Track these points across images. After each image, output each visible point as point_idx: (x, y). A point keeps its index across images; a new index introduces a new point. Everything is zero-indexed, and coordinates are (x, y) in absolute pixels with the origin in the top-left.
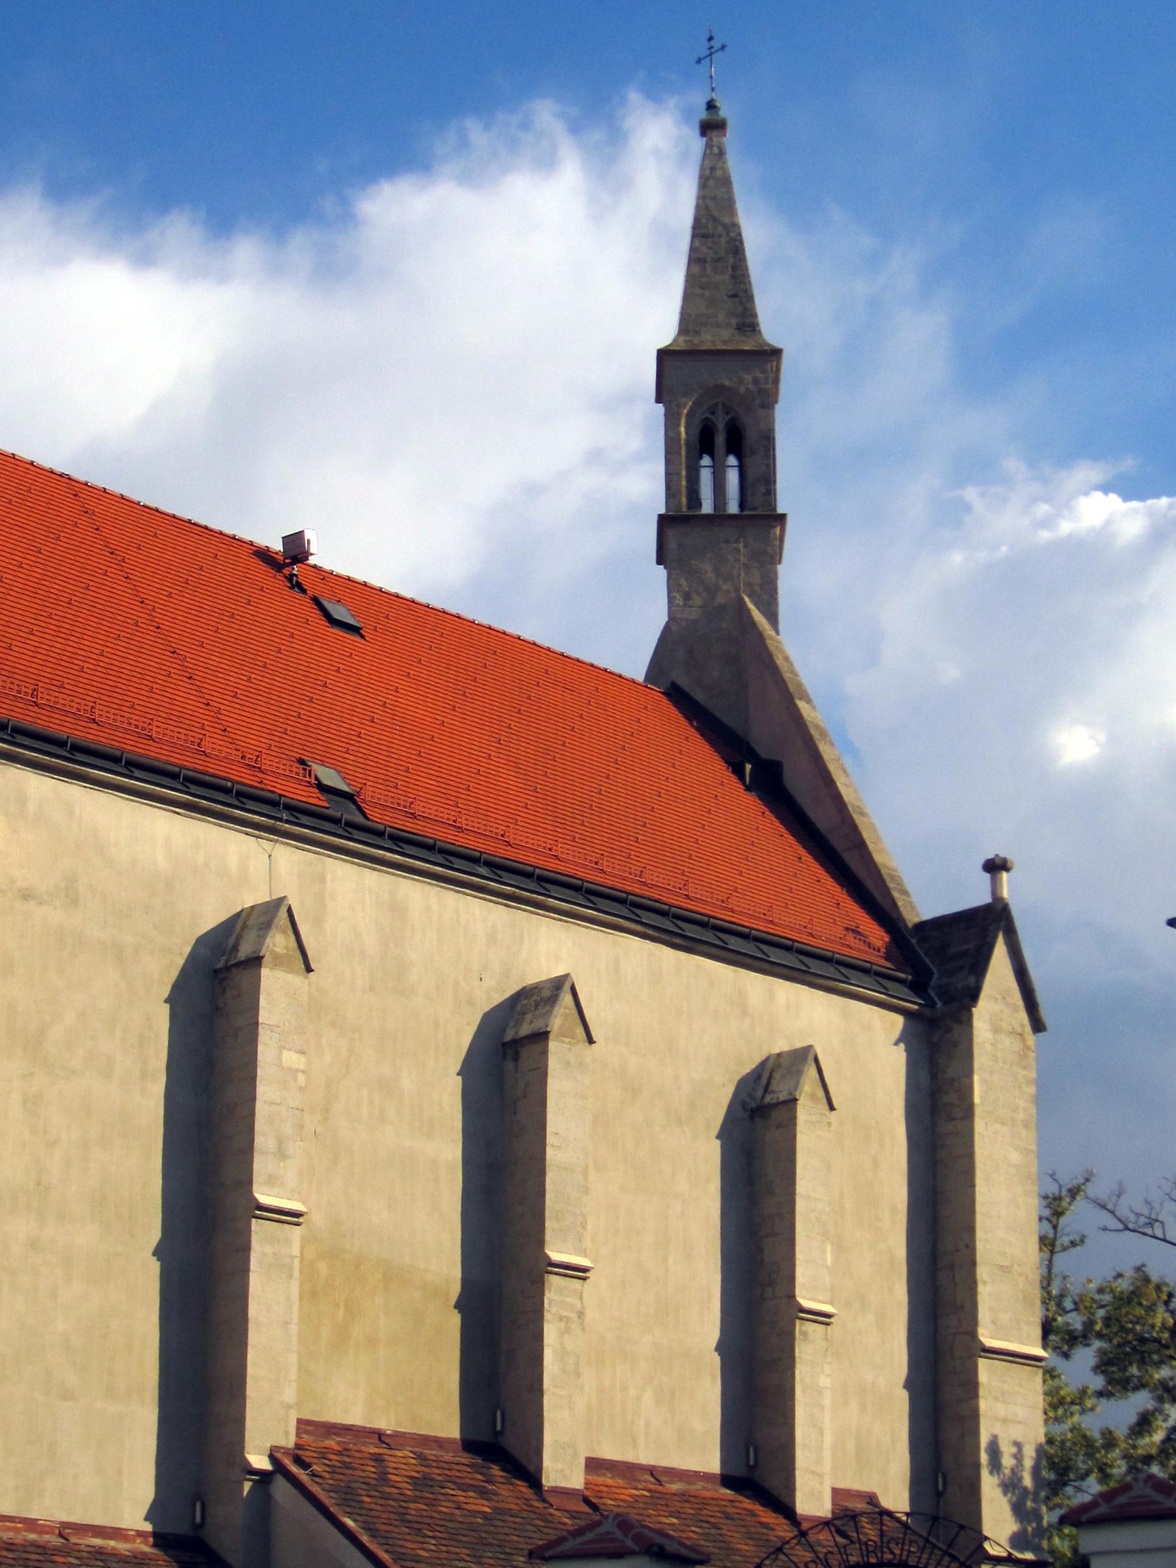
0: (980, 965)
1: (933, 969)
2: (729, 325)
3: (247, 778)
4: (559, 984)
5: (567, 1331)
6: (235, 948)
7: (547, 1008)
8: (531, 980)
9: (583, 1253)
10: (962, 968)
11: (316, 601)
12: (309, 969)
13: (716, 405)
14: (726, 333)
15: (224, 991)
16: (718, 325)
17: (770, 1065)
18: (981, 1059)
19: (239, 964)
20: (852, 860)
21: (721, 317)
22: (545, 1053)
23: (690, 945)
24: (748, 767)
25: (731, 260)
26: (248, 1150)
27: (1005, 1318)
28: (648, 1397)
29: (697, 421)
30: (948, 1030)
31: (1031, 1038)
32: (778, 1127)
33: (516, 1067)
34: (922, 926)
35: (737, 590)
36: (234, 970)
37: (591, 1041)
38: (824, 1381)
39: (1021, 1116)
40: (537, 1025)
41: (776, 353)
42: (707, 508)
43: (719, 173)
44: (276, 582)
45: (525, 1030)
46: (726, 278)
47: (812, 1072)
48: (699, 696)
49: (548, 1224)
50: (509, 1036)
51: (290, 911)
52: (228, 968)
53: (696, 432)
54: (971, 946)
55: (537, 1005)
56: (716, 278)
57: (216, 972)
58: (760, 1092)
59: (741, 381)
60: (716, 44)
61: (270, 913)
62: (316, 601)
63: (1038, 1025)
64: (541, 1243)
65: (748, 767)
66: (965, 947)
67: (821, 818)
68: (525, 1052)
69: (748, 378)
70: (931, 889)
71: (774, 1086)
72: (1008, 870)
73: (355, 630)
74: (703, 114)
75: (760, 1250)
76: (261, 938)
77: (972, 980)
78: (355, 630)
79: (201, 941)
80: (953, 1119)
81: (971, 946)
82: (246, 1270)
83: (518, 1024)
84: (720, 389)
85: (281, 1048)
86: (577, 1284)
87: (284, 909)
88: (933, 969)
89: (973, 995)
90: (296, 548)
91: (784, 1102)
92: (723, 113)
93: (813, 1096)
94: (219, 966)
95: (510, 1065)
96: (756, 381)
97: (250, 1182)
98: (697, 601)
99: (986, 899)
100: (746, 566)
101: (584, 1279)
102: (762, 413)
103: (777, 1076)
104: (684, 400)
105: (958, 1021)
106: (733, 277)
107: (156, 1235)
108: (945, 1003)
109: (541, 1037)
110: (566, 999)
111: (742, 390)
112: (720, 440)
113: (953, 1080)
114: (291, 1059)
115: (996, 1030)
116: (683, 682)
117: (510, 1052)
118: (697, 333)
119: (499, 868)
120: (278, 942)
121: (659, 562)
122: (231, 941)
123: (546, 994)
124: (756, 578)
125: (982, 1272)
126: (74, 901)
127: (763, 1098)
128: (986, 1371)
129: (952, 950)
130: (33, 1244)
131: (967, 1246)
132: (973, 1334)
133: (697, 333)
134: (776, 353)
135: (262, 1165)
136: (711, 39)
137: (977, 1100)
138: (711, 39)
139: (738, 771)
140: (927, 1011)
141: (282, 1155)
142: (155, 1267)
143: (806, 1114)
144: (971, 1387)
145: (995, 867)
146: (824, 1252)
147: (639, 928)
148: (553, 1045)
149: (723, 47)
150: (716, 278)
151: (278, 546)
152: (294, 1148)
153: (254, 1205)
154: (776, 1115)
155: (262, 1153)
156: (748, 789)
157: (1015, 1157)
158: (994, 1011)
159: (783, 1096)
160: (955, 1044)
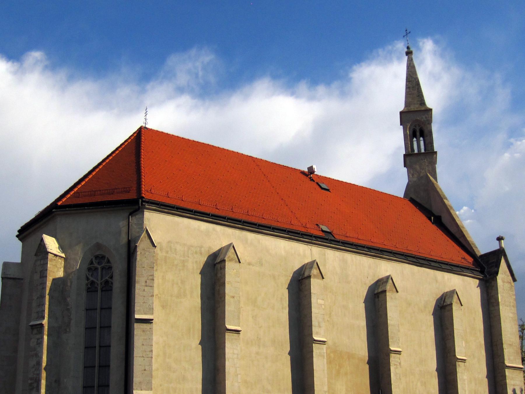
0: (498, 265)
1: (486, 267)
3: (303, 230)
4: (388, 278)
5: (396, 368)
6: (304, 274)
8: (381, 277)
9: (400, 347)
11: (317, 183)
12: (323, 278)
14: (417, 106)
16: (414, 104)
17: (444, 295)
18: (500, 290)
19: (305, 278)
20: (461, 240)
22: (386, 295)
23: (421, 265)
24: (432, 218)
25: (417, 87)
26: (311, 326)
27: (512, 358)
28: (419, 384)
29: (411, 129)
31: (513, 284)
34: (482, 256)
35: (426, 172)
37: (397, 292)
38: (465, 377)
39: (512, 304)
40: (383, 289)
41: (431, 110)
42: (416, 151)
43: (412, 65)
44: (307, 179)
45: (380, 290)
46: (416, 92)
47: (456, 296)
48: (418, 200)
49: (390, 340)
50: (376, 292)
51: (317, 263)
52: (302, 279)
53: (412, 132)
57: (299, 280)
58: (442, 302)
59: (422, 118)
60: (408, 31)
61: (312, 264)
62: (317, 183)
63: (514, 280)
64: (388, 345)
65: (432, 218)
67: (453, 230)
68: (380, 296)
69: (424, 117)
70: (483, 246)
71: (446, 300)
72: (503, 240)
73: (328, 190)
76: (310, 271)
77: (496, 269)
78: (328, 190)
82: (312, 357)
83: (378, 289)
84: (417, 120)
85: (317, 299)
86: (398, 355)
87: (315, 263)
88: (486, 267)
89: (497, 273)
90: (311, 170)
92: (411, 49)
93: (456, 303)
95: (377, 300)
96: (426, 118)
97: (312, 334)
98: (415, 176)
99: (498, 247)
102: (428, 125)
103: (447, 298)
106: (418, 91)
107: (288, 349)
109: (385, 292)
110: (390, 281)
111: (423, 120)
112: (418, 134)
114: (320, 301)
115: (503, 282)
116: (414, 197)
118: (410, 106)
119: (370, 249)
120: (315, 271)
121: (405, 166)
122: (303, 272)
123: (385, 280)
125: (505, 346)
126: (262, 265)
128: (508, 372)
130: (257, 353)
132: (504, 363)
134: (431, 110)
135: (315, 330)
137: (500, 301)
139: (430, 219)
140: (485, 278)
141: (320, 327)
142: (289, 357)
143: (455, 307)
144: (504, 377)
145: (500, 239)
146: (462, 343)
147: (408, 262)
148: (387, 294)
151: (306, 170)
152: (323, 324)
154: (448, 308)
155: (315, 326)
156: (433, 223)
157: (511, 315)
158: (502, 277)
159: (449, 303)
160: (493, 286)
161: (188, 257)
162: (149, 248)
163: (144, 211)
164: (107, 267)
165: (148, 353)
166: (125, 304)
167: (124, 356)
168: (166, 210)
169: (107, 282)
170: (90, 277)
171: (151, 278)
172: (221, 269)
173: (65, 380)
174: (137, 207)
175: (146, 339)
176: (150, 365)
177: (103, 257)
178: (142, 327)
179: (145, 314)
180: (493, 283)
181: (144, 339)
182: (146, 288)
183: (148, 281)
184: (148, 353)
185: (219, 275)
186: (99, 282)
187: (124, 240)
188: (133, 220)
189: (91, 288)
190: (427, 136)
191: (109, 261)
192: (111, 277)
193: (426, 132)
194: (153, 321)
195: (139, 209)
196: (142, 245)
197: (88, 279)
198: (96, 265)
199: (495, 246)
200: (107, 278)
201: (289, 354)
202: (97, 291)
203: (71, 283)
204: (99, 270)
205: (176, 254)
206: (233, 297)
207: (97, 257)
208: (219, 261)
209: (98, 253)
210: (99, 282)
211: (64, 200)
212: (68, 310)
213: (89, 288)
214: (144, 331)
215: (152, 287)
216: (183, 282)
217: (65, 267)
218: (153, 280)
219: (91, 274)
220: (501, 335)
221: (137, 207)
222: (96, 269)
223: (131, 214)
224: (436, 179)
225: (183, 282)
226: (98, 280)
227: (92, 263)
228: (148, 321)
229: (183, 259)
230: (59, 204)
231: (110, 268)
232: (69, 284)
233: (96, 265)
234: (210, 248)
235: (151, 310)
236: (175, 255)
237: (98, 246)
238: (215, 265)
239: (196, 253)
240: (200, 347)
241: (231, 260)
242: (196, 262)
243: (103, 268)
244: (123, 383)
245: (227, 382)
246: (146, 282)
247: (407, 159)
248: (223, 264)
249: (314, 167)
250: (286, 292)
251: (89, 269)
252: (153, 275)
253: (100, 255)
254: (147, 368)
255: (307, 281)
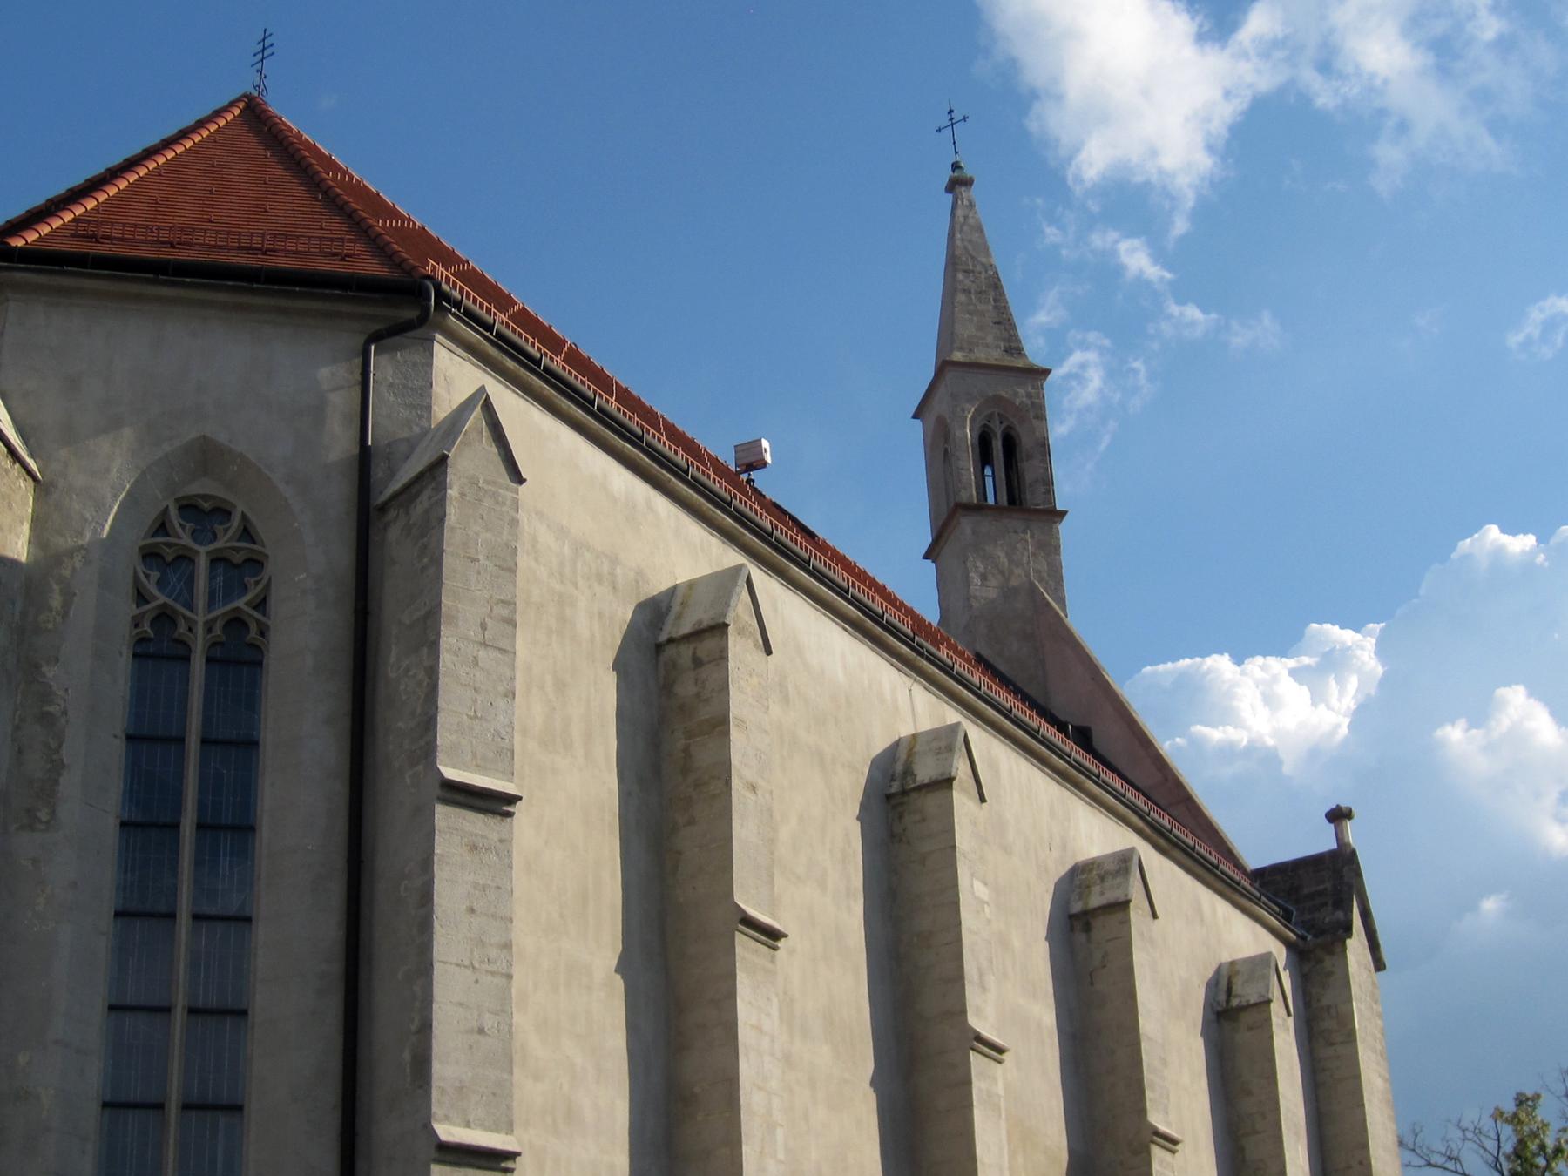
2: (998, 347)
6: (908, 772)
7: (1118, 880)
9: (1169, 1124)
10: (1325, 904)
12: (982, 799)
13: (992, 414)
15: (901, 817)
16: (987, 346)
17: (1225, 972)
21: (990, 339)
25: (992, 294)
26: (958, 978)
29: (977, 426)
30: (1321, 961)
32: (1250, 1029)
33: (1089, 940)
35: (1028, 575)
36: (914, 795)
37: (1155, 916)
42: (991, 501)
43: (971, 221)
45: (1095, 901)
49: (1148, 1093)
50: (1077, 907)
52: (905, 792)
53: (976, 437)
54: (1328, 885)
55: (1102, 879)
56: (980, 307)
57: (889, 797)
58: (1222, 997)
59: (1016, 394)
60: (957, 116)
64: (1142, 1111)
66: (1321, 887)
68: (1097, 923)
69: (1021, 392)
71: (1237, 989)
74: (947, 174)
75: (1241, 1149)
77: (1340, 915)
79: (875, 763)
80: (1332, 1044)
81: (1328, 885)
82: (969, 1106)
84: (997, 400)
91: (1256, 1005)
92: (968, 171)
94: (893, 790)
95: (1080, 937)
96: (1029, 395)
97: (964, 1012)
99: (1333, 845)
100: (1034, 554)
101: (1173, 1152)
102: (1036, 423)
104: (967, 406)
105: (1331, 953)
106: (996, 307)
108: (1315, 936)
112: (997, 446)
113: (1329, 1007)
116: (985, 653)
117: (1078, 925)
118: (971, 351)
122: (899, 768)
123: (1112, 867)
124: (1044, 567)
127: (1228, 1001)
129: (1306, 891)
131: (1361, 1163)
133: (971, 351)
135: (972, 996)
136: (951, 112)
138: (951, 112)
140: (1301, 943)
141: (983, 988)
147: (1140, 823)
149: (965, 119)
150: (980, 307)
152: (991, 980)
153: (972, 1036)
154: (1246, 1018)
159: (1253, 999)
160: (1330, 974)
161: (576, 585)
162: (494, 483)
163: (432, 339)
164: (238, 558)
165: (493, 953)
166: (345, 724)
167: (337, 968)
168: (510, 364)
169: (236, 622)
170: (154, 590)
171: (505, 612)
172: (697, 663)
173: (22, 1059)
174: (411, 314)
175: (484, 887)
176: (503, 1006)
177: (222, 512)
178: (468, 827)
179: (481, 769)
180: (1328, 962)
181: (475, 885)
182: (482, 653)
183: (489, 622)
184: (493, 953)
185: (686, 688)
186: (200, 618)
187: (339, 443)
188: (383, 367)
189: (158, 647)
190: (1029, 457)
191: (247, 533)
192: (261, 604)
193: (1025, 441)
194: (518, 809)
195: (423, 320)
196: (470, 462)
197: (141, 597)
198: (186, 540)
199: (1322, 841)
200: (240, 603)
201: (873, 1083)
202: (186, 659)
203: (68, 596)
204: (202, 563)
205: (536, 560)
206: (754, 789)
207: (188, 507)
208: (686, 629)
209: (195, 488)
210: (200, 618)
211: (32, 237)
212: (46, 719)
213: (142, 640)
214: (474, 848)
215: (509, 652)
216: (561, 686)
217: (37, 522)
218: (512, 623)
219: (155, 575)
220: (1364, 1146)
221: (411, 314)
222: (185, 558)
223: (376, 338)
224: (1062, 601)
225: (561, 686)
226: (190, 606)
227: (162, 527)
228: (495, 804)
229: (558, 587)
230: (18, 242)
231: (256, 563)
232: (56, 601)
233: (186, 540)
234: (640, 573)
235: (504, 757)
236: (533, 564)
237: (207, 455)
238: (659, 647)
239: (599, 578)
240: (619, 982)
241: (741, 632)
242: (601, 615)
243: (217, 560)
244: (330, 1094)
245: (746, 1149)
246: (484, 627)
247: (966, 526)
248: (707, 646)
249: (765, 444)
250: (856, 828)
251: (150, 555)
252: (510, 603)
253: (205, 497)
254: (489, 1022)
255: (931, 802)
